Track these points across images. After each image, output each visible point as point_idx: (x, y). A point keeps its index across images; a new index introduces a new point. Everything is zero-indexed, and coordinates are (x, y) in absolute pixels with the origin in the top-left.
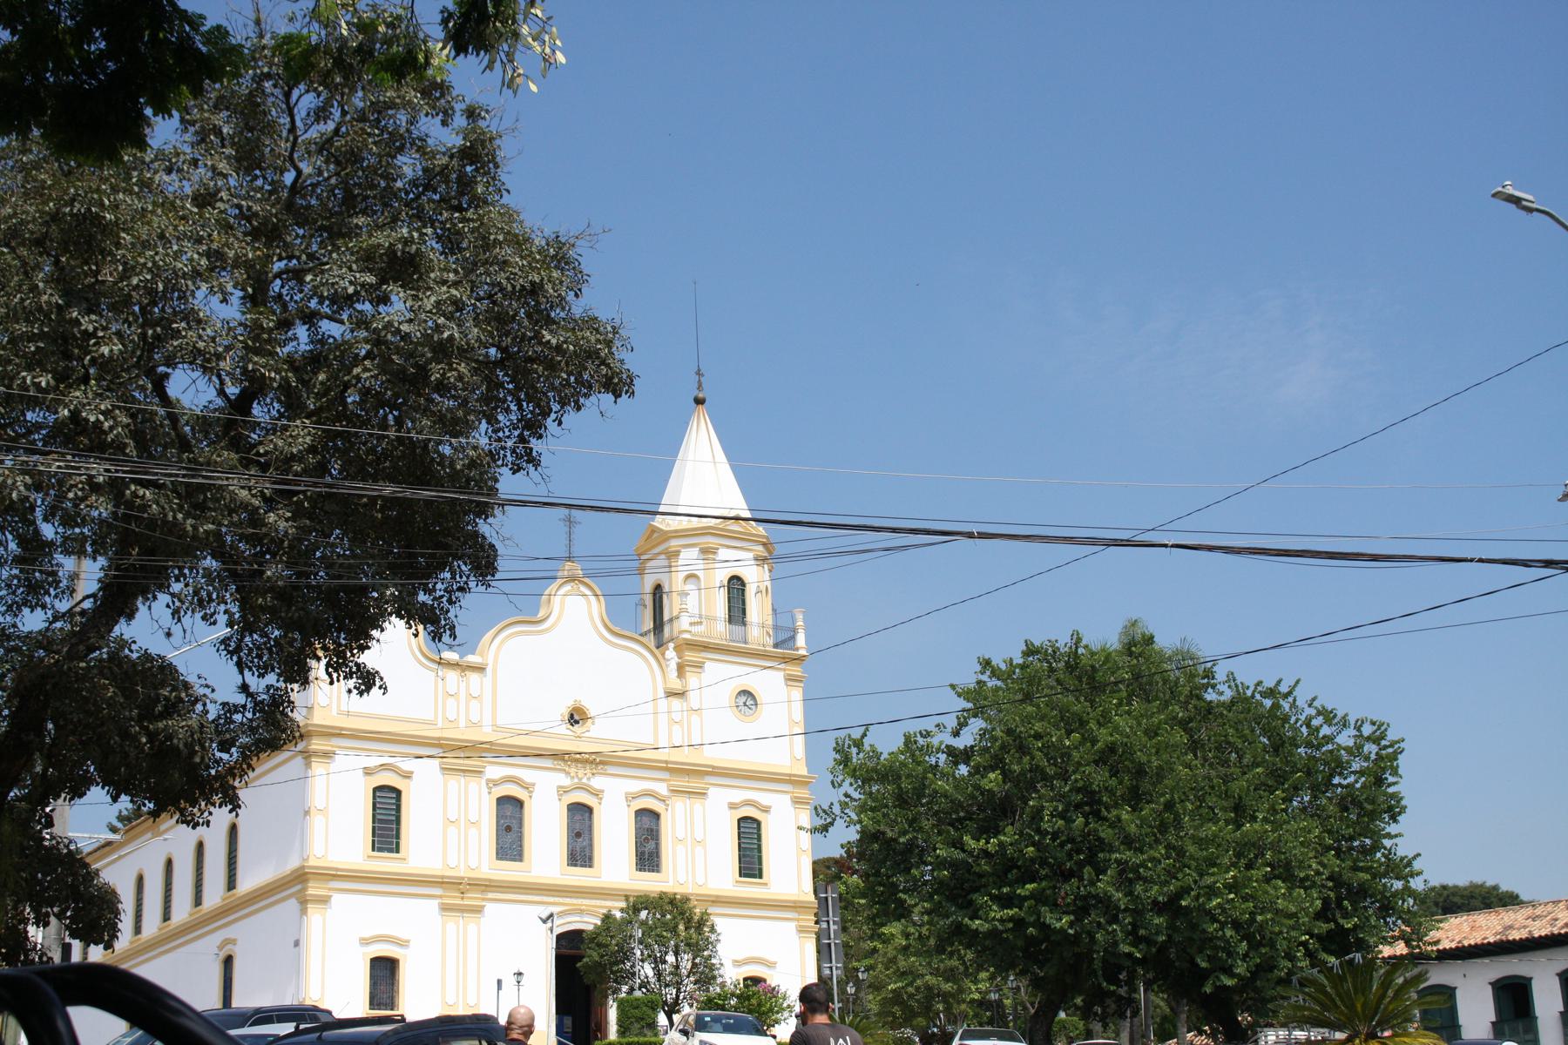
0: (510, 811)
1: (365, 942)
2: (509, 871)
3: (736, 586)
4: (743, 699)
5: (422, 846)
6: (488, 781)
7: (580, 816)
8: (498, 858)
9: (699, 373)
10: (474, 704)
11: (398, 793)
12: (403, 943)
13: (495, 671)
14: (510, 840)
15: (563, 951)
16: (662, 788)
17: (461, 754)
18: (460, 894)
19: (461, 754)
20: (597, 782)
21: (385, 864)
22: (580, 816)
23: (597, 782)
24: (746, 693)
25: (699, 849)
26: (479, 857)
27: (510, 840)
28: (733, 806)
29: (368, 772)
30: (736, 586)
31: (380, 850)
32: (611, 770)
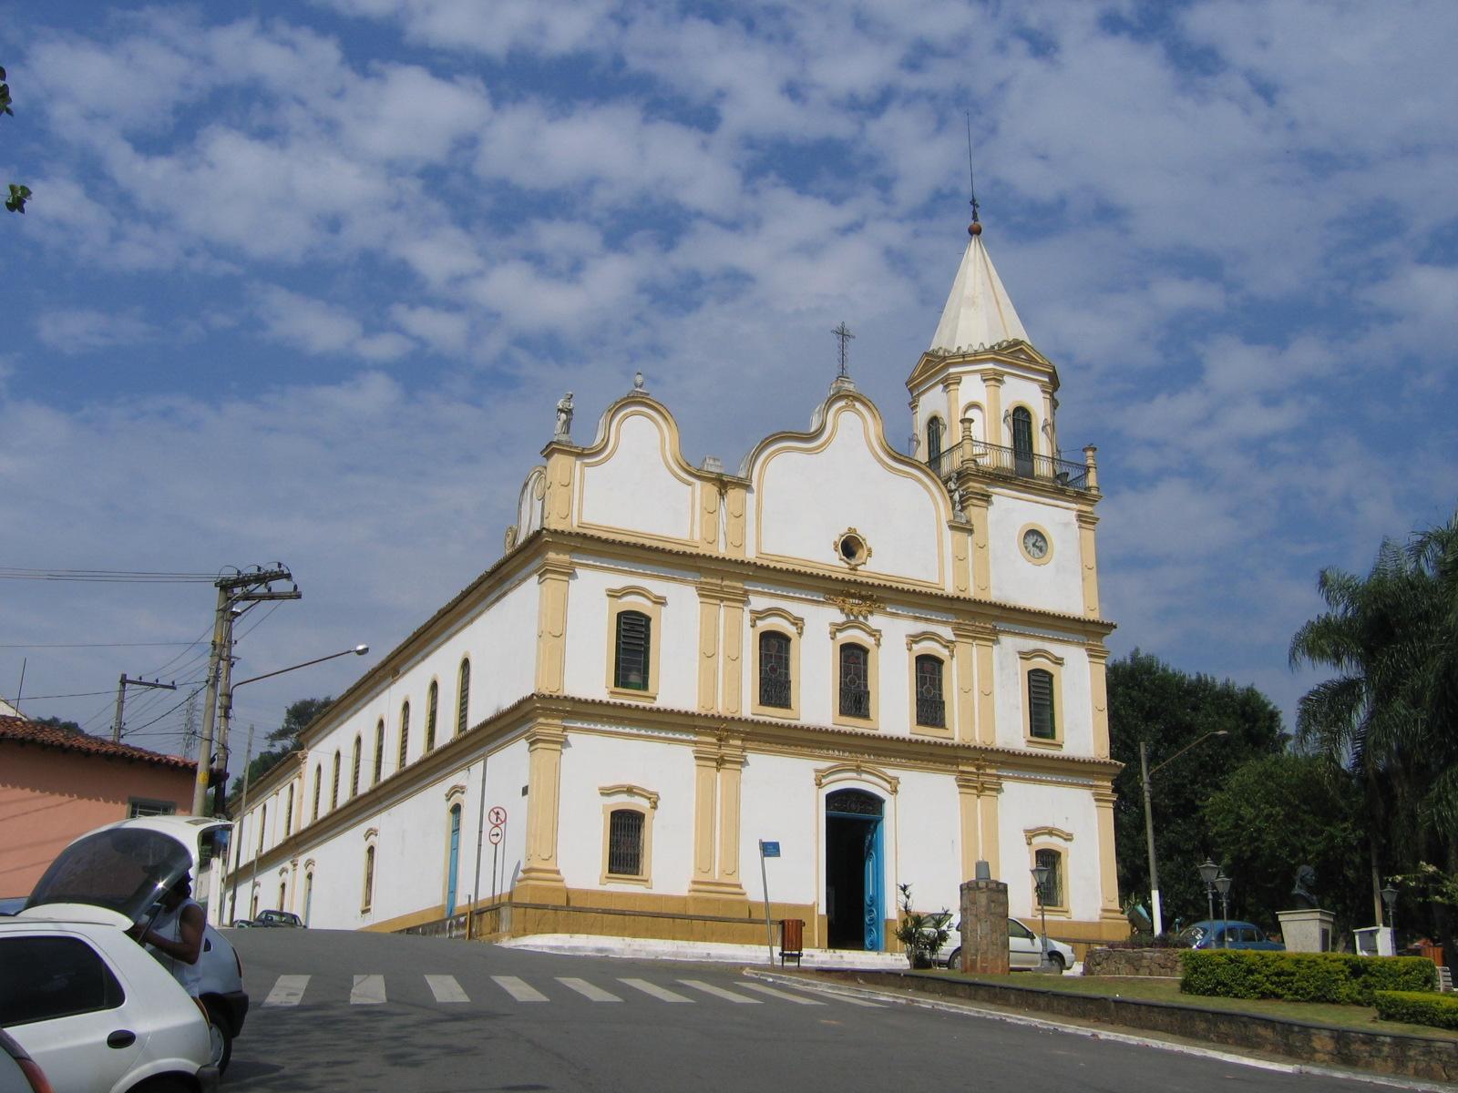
0: (775, 650)
1: (606, 792)
3: (1021, 418)
4: (1031, 540)
5: (675, 682)
6: (752, 612)
7: (854, 661)
8: (761, 703)
14: (775, 687)
15: (836, 813)
17: (721, 575)
18: (720, 737)
19: (721, 575)
20: (876, 621)
21: (630, 699)
22: (854, 661)
24: (1033, 533)
30: (1021, 418)
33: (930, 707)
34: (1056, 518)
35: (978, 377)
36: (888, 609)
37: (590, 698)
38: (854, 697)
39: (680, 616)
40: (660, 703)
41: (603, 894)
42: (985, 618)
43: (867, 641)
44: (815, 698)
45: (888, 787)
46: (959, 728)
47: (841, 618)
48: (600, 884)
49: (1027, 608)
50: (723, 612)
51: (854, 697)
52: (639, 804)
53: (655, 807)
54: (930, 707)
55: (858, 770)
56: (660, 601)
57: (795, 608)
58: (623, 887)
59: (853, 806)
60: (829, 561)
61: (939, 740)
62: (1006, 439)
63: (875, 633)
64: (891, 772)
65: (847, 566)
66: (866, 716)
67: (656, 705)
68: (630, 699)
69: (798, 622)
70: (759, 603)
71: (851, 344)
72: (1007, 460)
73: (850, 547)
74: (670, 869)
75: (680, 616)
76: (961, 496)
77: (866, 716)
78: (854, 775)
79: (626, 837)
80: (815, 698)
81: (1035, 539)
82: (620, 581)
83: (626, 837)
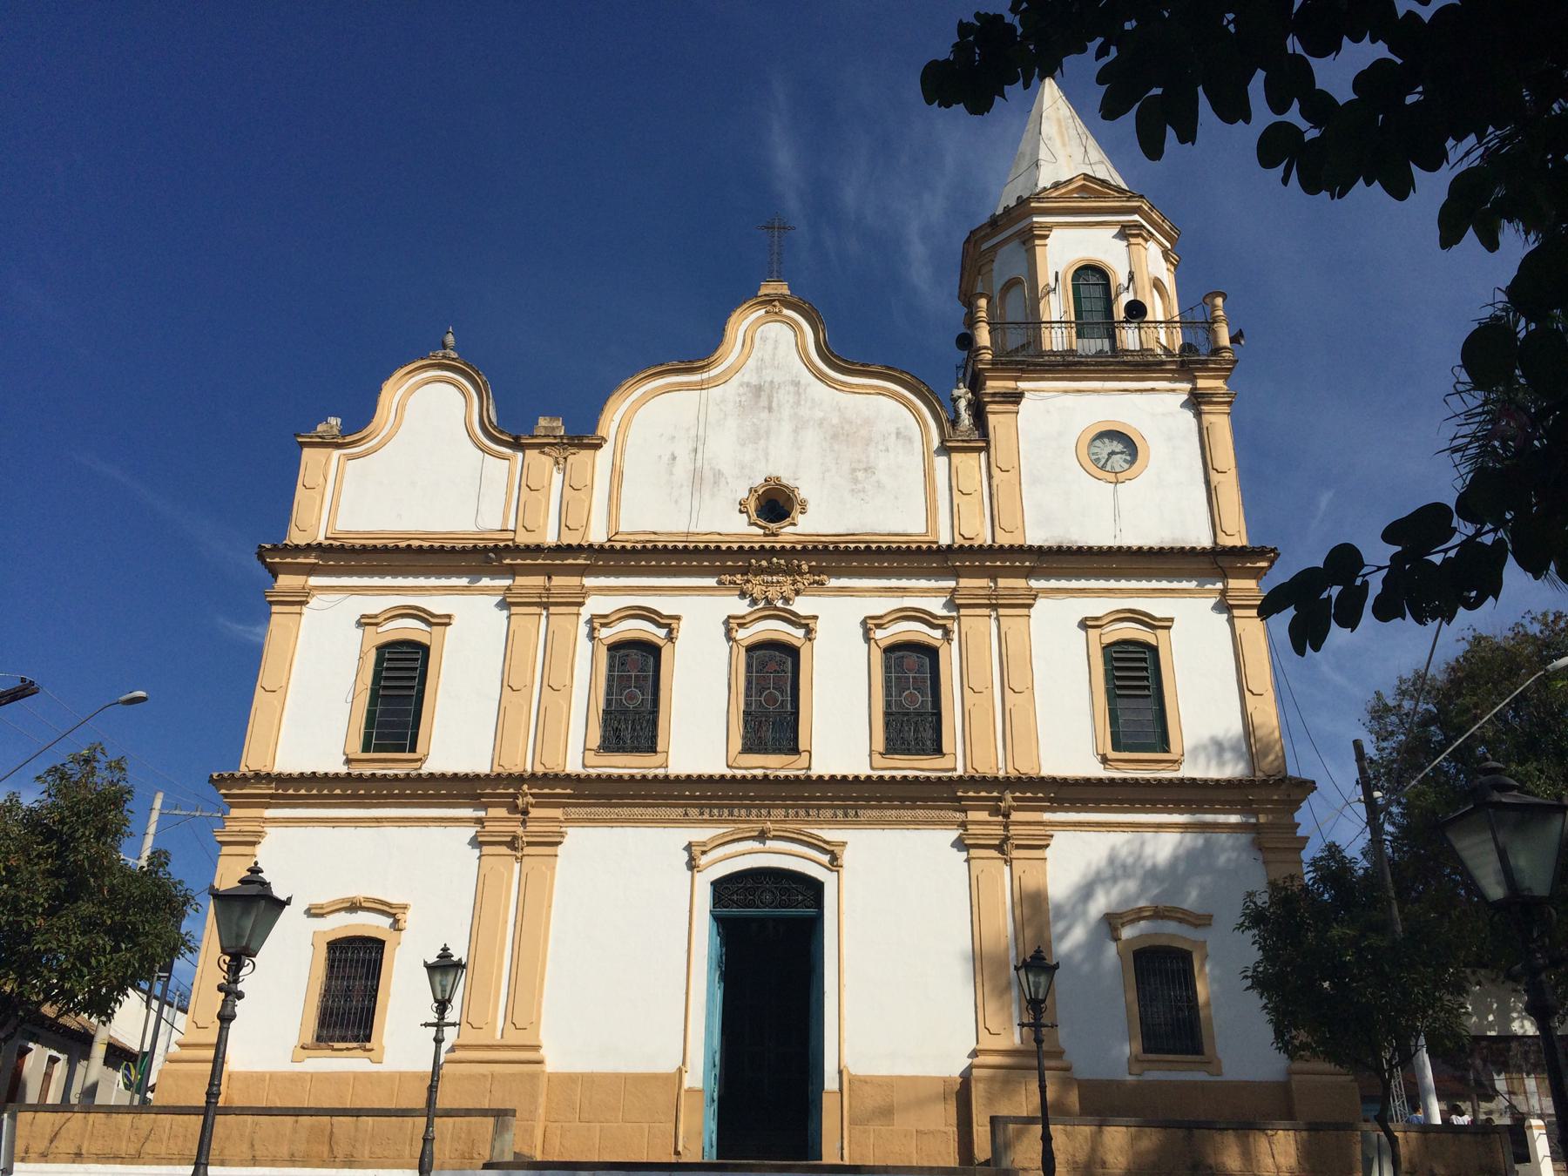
15: (735, 911)
16: (936, 606)
21: (394, 766)
29: (366, 622)
31: (379, 749)
32: (834, 582)
34: (1156, 412)
35: (1014, 244)
37: (296, 771)
39: (472, 633)
40: (429, 767)
41: (295, 1079)
42: (1005, 568)
43: (794, 635)
44: (699, 729)
45: (825, 859)
46: (967, 748)
47: (741, 607)
49: (1065, 545)
50: (534, 626)
52: (369, 924)
53: (396, 926)
55: (762, 836)
56: (445, 621)
59: (768, 897)
60: (729, 522)
61: (933, 775)
63: (806, 625)
64: (830, 834)
65: (761, 531)
66: (795, 750)
67: (426, 769)
68: (394, 766)
69: (669, 624)
73: (775, 504)
75: (472, 633)
77: (795, 750)
78: (756, 845)
80: (699, 729)
81: (1117, 447)
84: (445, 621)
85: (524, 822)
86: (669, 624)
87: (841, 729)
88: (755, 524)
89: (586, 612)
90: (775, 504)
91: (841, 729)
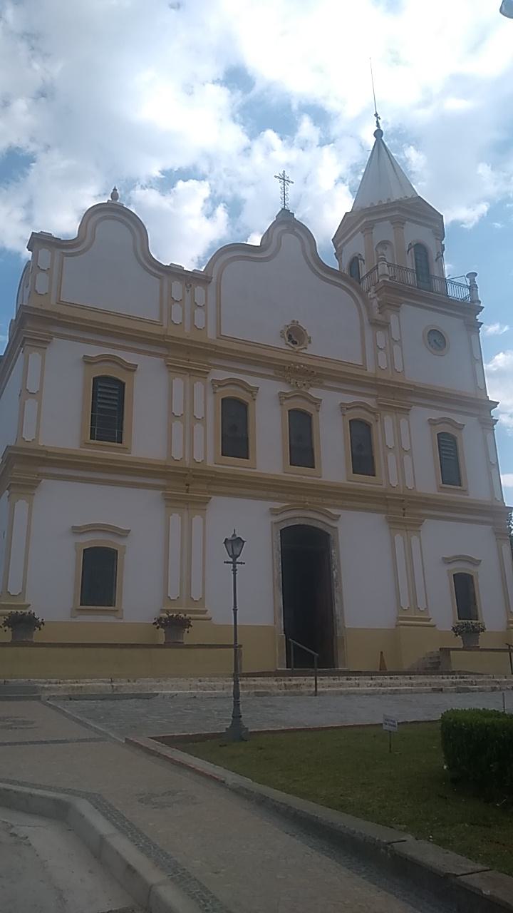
1: (77, 531)
2: (233, 466)
5: (146, 436)
9: (376, 115)
10: (198, 312)
11: (121, 385)
12: (124, 534)
13: (219, 285)
14: (235, 438)
16: (371, 402)
20: (315, 392)
21: (106, 452)
23: (315, 392)
25: (406, 457)
26: (204, 448)
27: (235, 438)
28: (432, 422)
29: (88, 361)
32: (326, 383)
33: (363, 460)
36: (326, 384)
38: (302, 449)
43: (308, 408)
48: (71, 617)
51: (302, 449)
54: (363, 460)
56: (132, 369)
57: (251, 381)
58: (97, 619)
62: (410, 263)
63: (316, 403)
64: (334, 512)
69: (253, 391)
70: (222, 375)
71: (290, 187)
72: (411, 278)
73: (295, 335)
74: (139, 598)
76: (379, 303)
79: (99, 575)
82: (94, 351)
83: (99, 575)
84: (132, 369)
85: (187, 491)
86: (253, 391)
87: (333, 458)
88: (287, 344)
89: (210, 379)
90: (295, 335)
91: (333, 458)
